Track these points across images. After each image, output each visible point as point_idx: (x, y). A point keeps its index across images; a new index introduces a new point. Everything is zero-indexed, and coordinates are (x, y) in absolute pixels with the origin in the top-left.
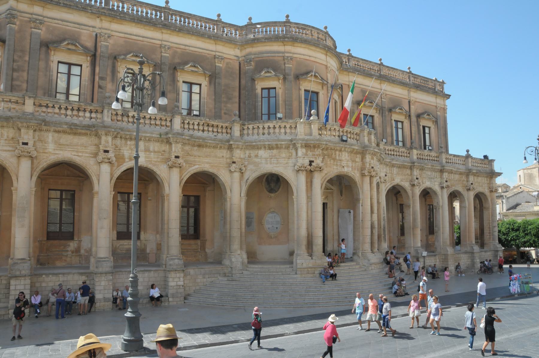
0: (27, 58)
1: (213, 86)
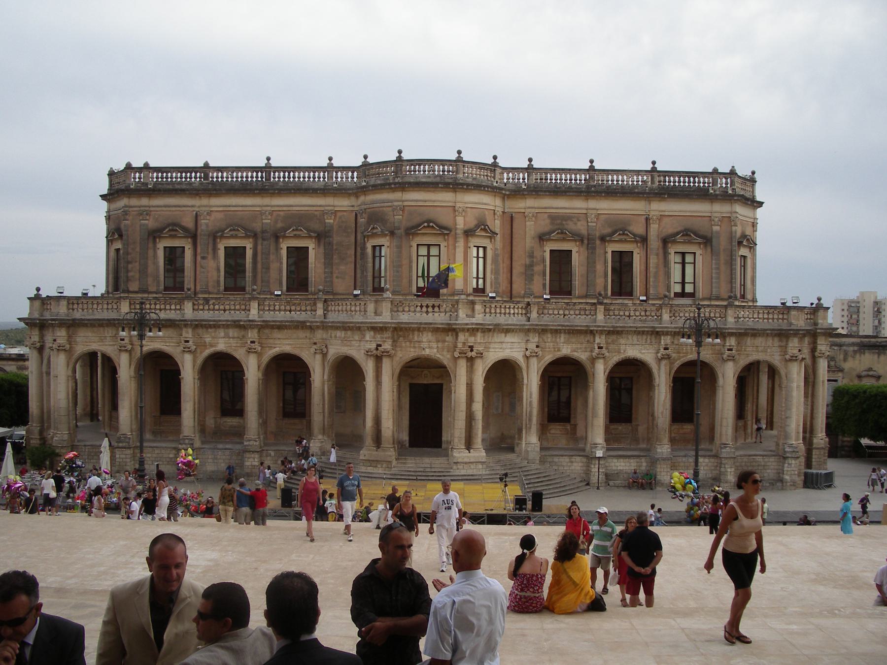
0: (138, 249)
1: (322, 247)
